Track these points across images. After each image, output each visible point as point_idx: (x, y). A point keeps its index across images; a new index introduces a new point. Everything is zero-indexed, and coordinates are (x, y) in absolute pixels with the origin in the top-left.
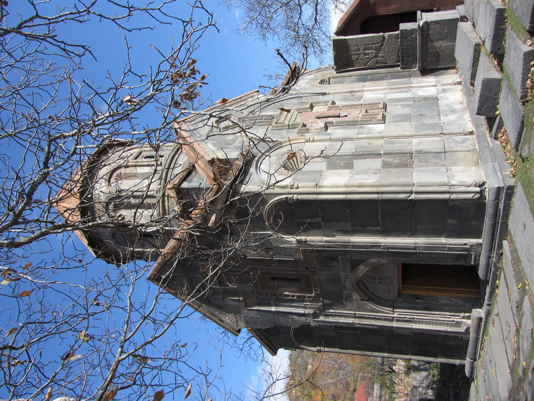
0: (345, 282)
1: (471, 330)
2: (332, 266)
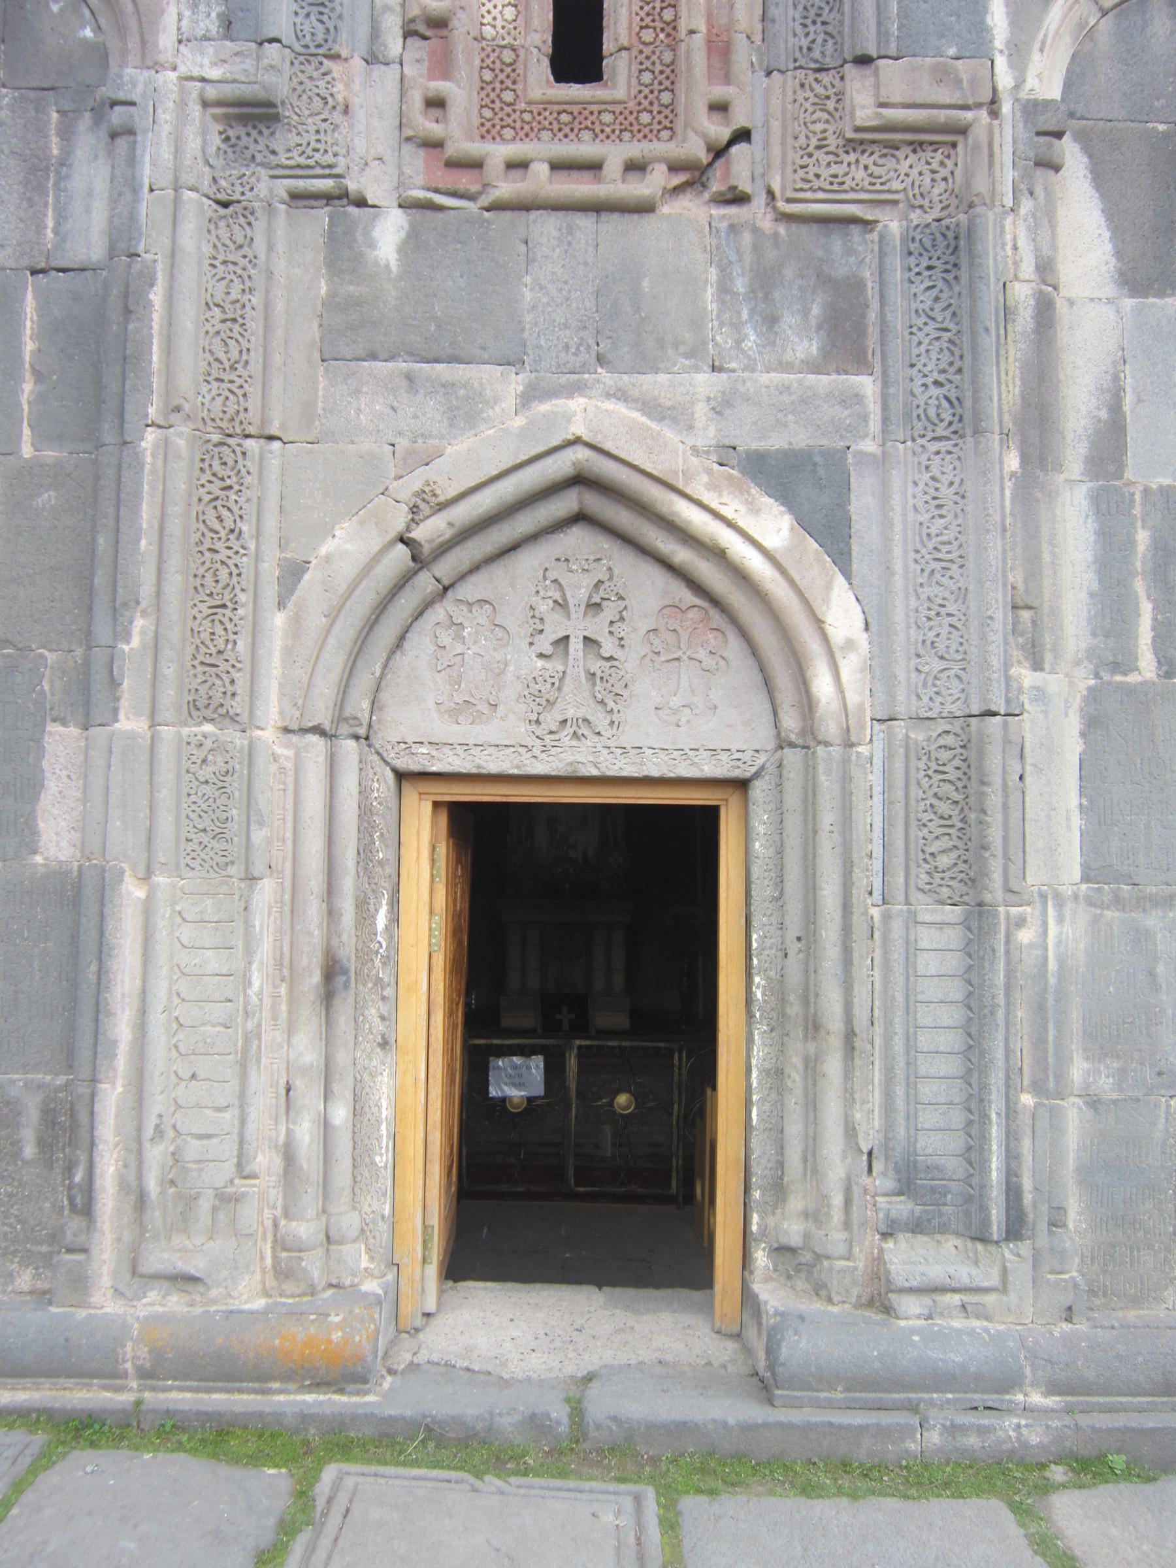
0: (620, 395)
2: (771, 321)
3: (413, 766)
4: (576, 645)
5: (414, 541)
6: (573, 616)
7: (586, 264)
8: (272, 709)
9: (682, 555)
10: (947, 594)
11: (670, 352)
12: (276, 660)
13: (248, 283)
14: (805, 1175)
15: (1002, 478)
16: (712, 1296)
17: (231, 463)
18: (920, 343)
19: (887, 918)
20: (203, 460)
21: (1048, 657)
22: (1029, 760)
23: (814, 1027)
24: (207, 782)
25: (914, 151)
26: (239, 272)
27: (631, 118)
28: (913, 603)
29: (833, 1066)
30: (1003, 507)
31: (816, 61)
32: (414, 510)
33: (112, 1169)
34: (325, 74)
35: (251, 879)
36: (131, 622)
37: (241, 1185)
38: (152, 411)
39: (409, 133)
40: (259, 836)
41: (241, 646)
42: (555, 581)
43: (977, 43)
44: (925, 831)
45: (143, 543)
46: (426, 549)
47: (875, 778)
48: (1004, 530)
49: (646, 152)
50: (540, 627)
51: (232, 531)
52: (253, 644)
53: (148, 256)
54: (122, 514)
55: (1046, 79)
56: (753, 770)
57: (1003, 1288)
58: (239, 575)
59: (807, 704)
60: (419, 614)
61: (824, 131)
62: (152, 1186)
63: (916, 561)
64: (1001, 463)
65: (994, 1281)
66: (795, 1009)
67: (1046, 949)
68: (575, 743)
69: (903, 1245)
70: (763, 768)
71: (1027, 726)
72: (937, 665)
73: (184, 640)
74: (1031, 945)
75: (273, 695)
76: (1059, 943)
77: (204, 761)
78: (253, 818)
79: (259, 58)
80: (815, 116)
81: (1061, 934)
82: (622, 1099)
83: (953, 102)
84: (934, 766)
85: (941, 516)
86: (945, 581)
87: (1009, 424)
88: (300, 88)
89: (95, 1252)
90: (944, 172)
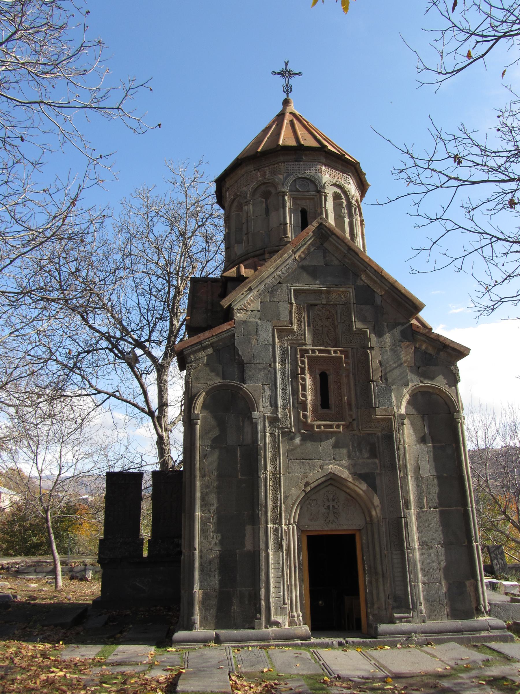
0: (337, 465)
1: (275, 628)
2: (361, 451)
4: (331, 507)
9: (348, 491)
23: (376, 573)
29: (381, 580)
37: (285, 606)
43: (391, 405)
47: (384, 529)
55: (403, 411)
57: (412, 618)
59: (371, 516)
82: (320, 602)
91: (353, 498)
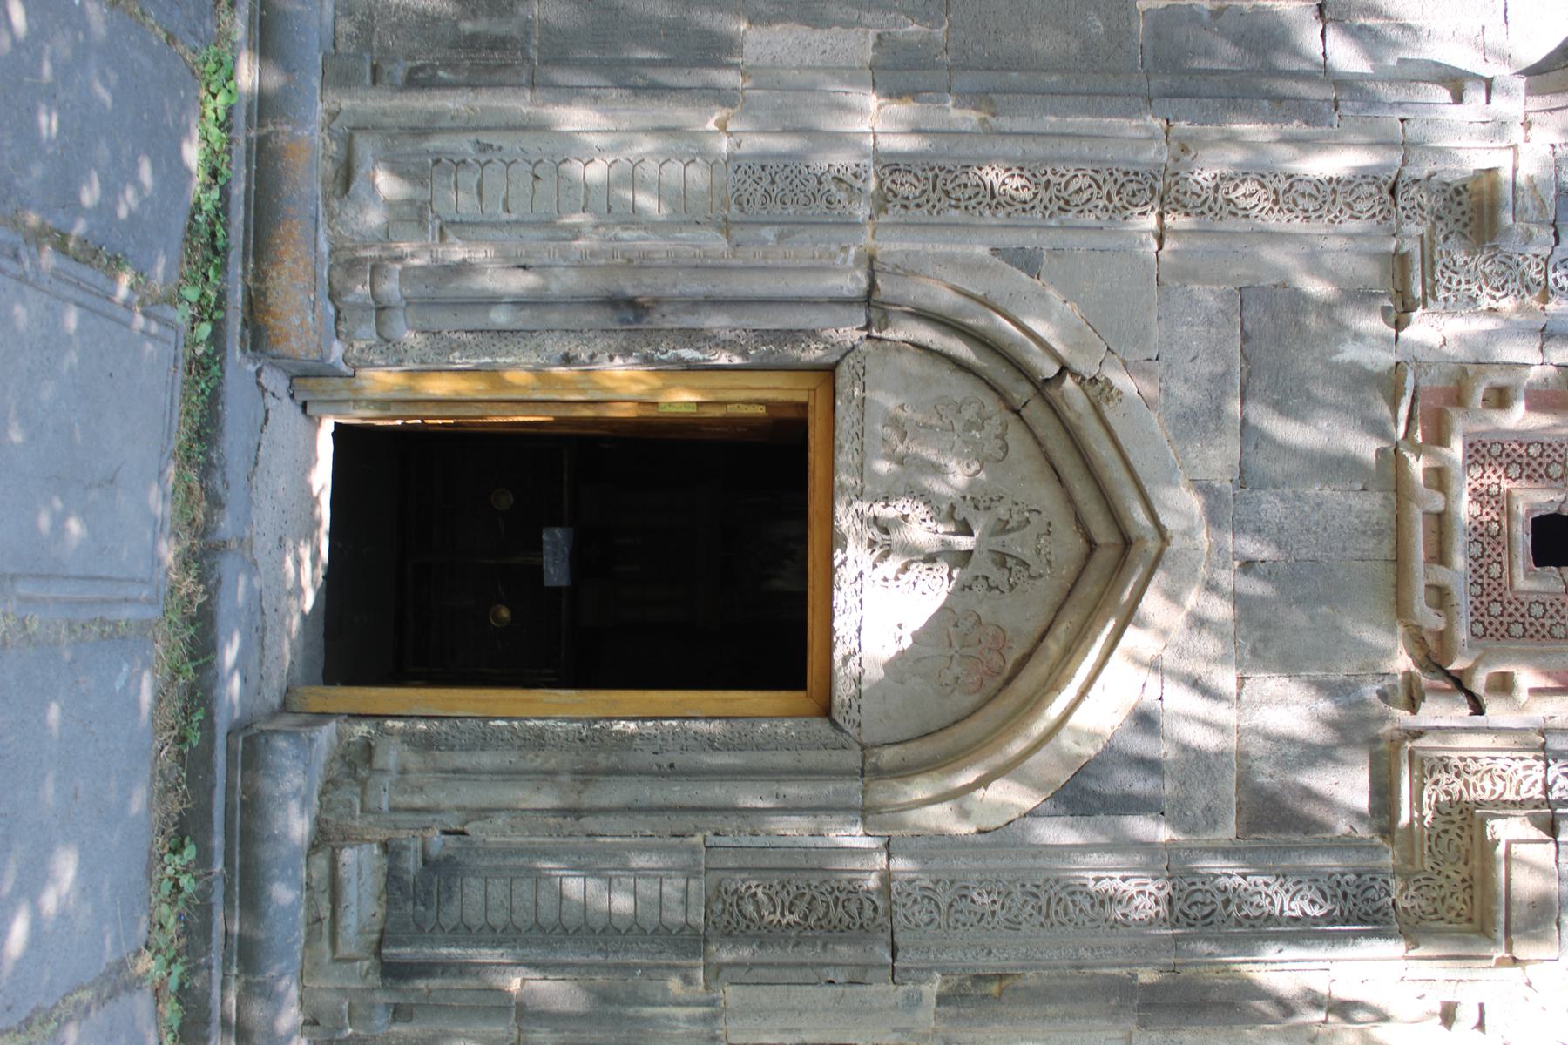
3: (840, 383)
5: (1063, 380)
6: (993, 540)
7: (1344, 549)
8: (893, 246)
9: (1053, 646)
10: (1015, 911)
11: (1257, 634)
12: (940, 248)
13: (1314, 215)
14: (442, 771)
15: (1130, 965)
16: (318, 684)
17: (1134, 201)
18: (1267, 885)
19: (693, 850)
20: (1136, 174)
21: (951, 1011)
22: (848, 989)
24: (820, 183)
25: (1464, 881)
26: (1326, 207)
27: (1495, 595)
28: (1007, 876)
30: (1101, 966)
31: (1554, 782)
32: (1094, 381)
33: (450, 105)
34: (1527, 287)
35: (725, 226)
36: (975, 109)
38: (1183, 124)
39: (1471, 370)
40: (768, 233)
41: (954, 213)
42: (1028, 521)
44: (778, 888)
45: (1052, 119)
46: (1052, 392)
48: (1078, 968)
49: (1457, 609)
50: (981, 506)
51: (1067, 202)
52: (957, 225)
53: (1336, 119)
54: (1080, 98)
56: (840, 721)
58: (1024, 210)
59: (905, 771)
60: (992, 387)
61: (1483, 790)
62: (436, 143)
63: (1047, 880)
64: (1146, 965)
65: (343, 951)
66: (602, 760)
67: (663, 1005)
68: (866, 541)
69: (377, 863)
70: (842, 731)
71: (882, 987)
72: (943, 901)
73: (959, 158)
74: (666, 990)
75: (906, 246)
76: (668, 1018)
77: (841, 180)
78: (785, 228)
79: (1539, 223)
80: (1497, 780)
81: (677, 1020)
83: (1513, 919)
84: (843, 897)
85: (1092, 906)
86: (1028, 909)
87: (1186, 972)
88: (1512, 264)
89: (373, 92)
90: (1442, 911)
91: (1009, 681)
